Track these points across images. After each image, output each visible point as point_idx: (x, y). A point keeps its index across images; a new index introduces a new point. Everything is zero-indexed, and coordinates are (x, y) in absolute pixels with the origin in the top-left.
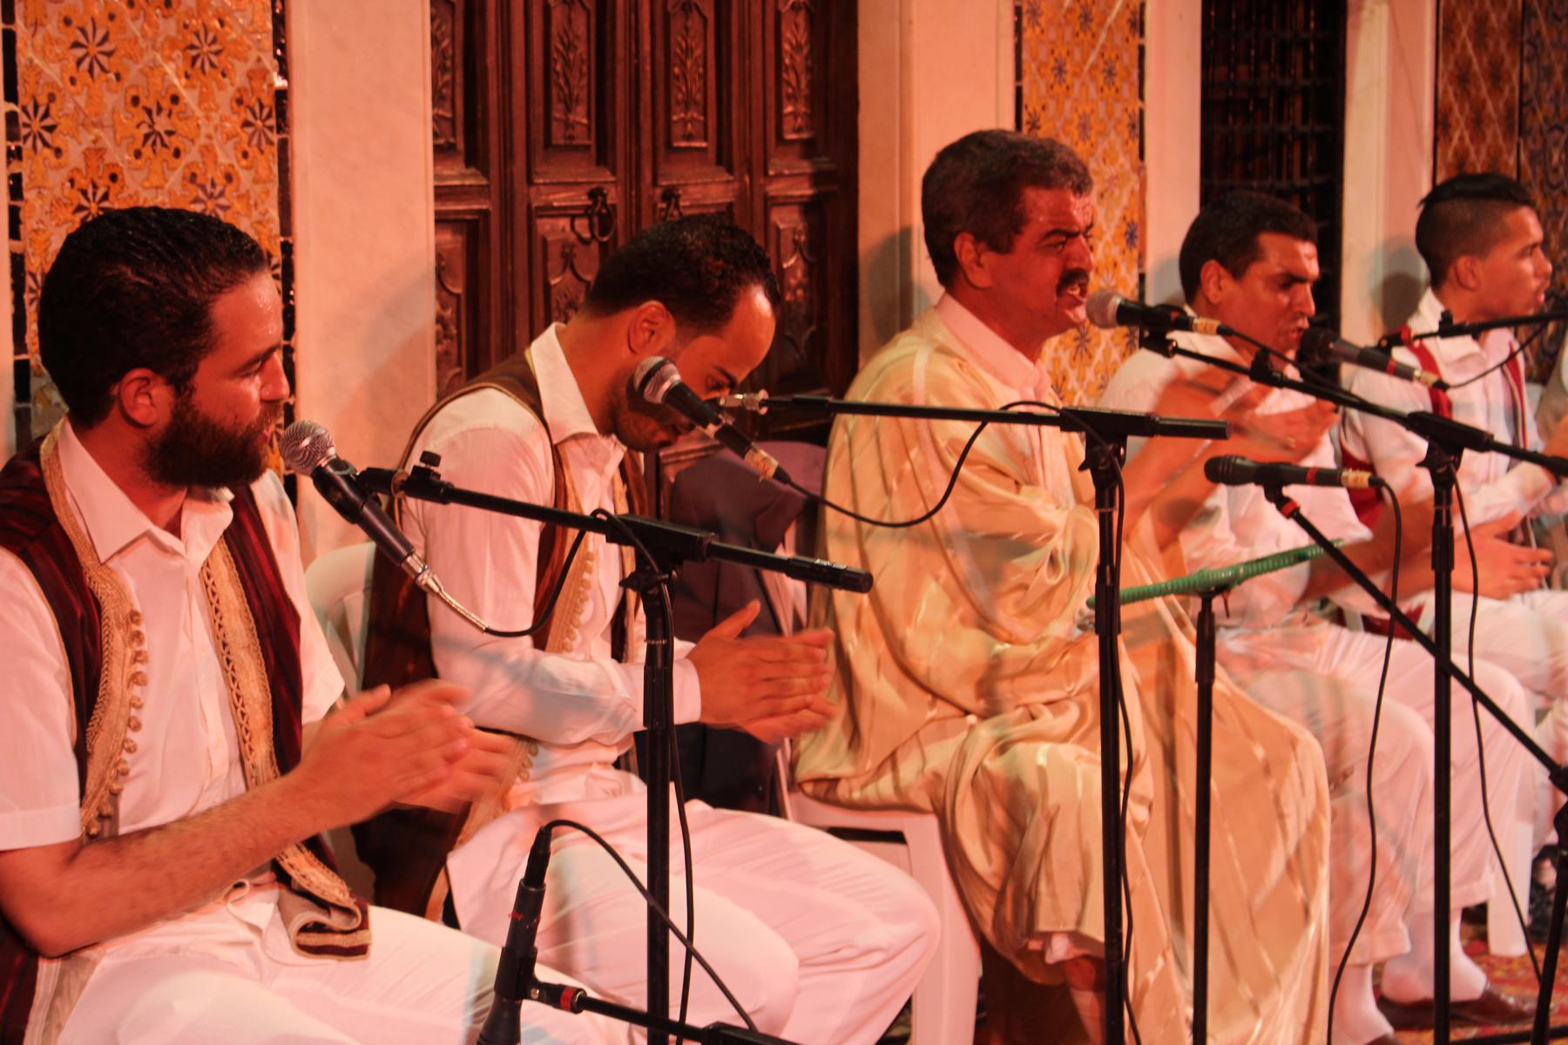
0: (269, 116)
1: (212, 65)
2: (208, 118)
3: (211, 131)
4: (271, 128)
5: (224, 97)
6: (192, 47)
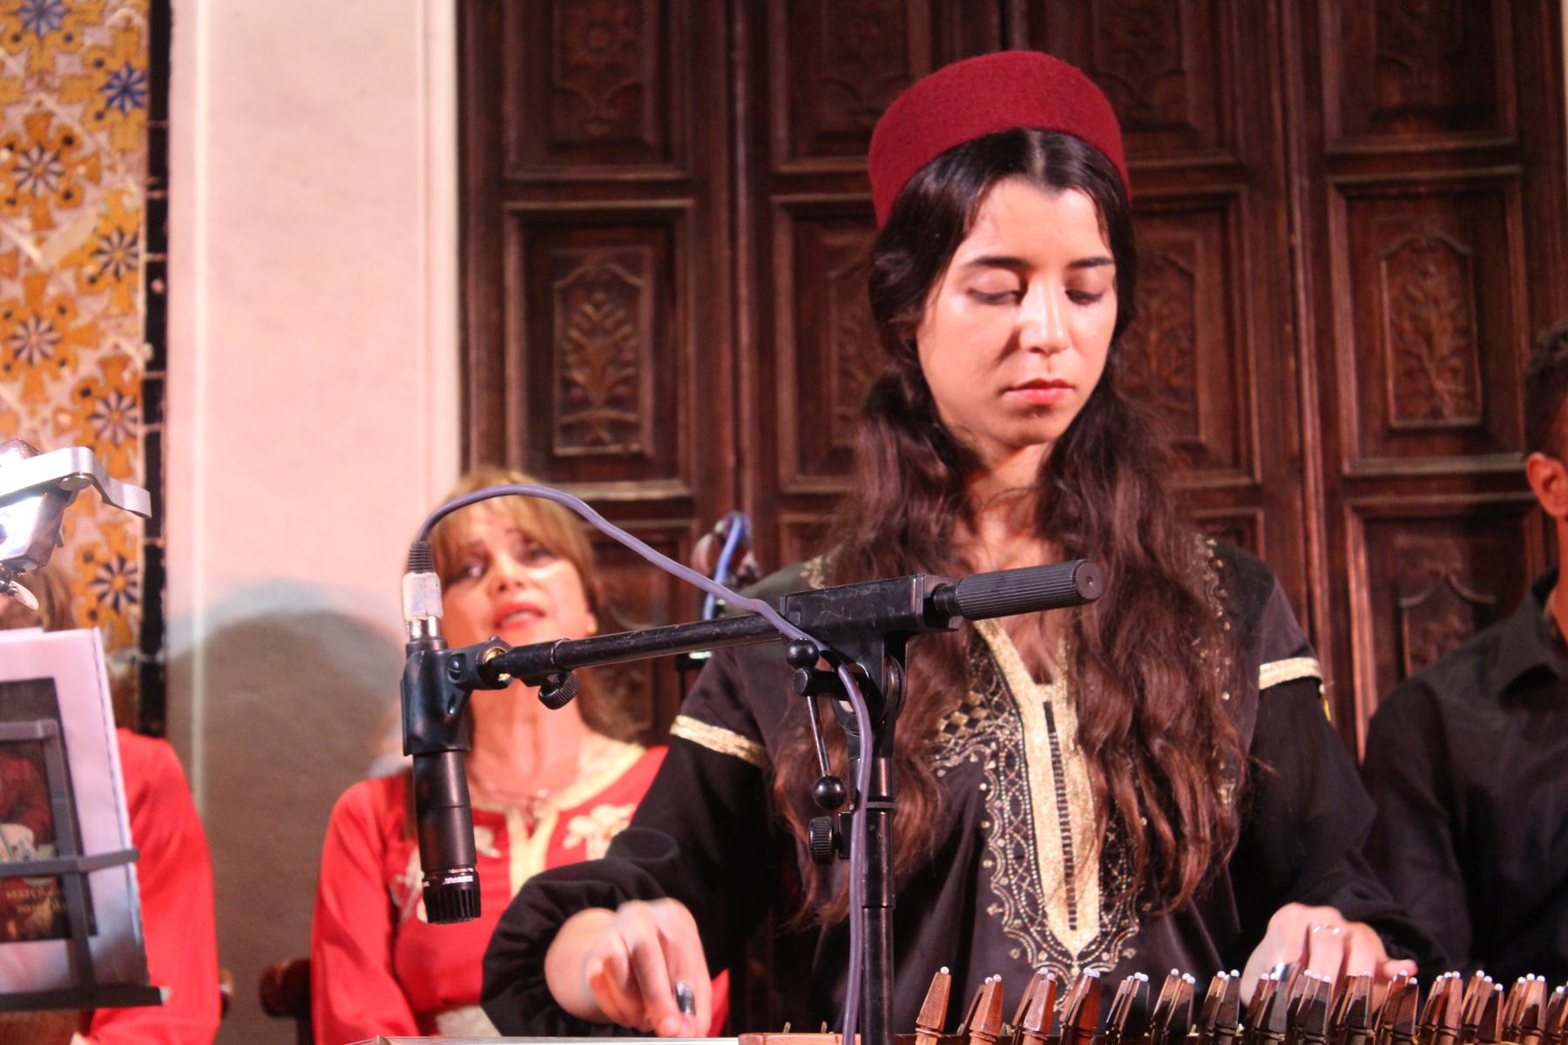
0: (133, 405)
1: (45, 356)
2: (32, 413)
3: (36, 423)
4: (135, 420)
5: (61, 389)
6: (15, 337)
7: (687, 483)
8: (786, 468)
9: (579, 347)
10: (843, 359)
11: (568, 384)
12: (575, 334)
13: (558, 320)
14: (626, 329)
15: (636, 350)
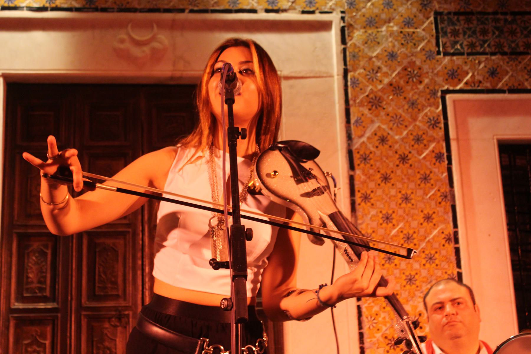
7: (58, 304)
8: (84, 300)
9: (31, 268)
10: (99, 272)
11: (28, 277)
12: (30, 264)
13: (26, 261)
14: (44, 263)
15: (46, 269)
